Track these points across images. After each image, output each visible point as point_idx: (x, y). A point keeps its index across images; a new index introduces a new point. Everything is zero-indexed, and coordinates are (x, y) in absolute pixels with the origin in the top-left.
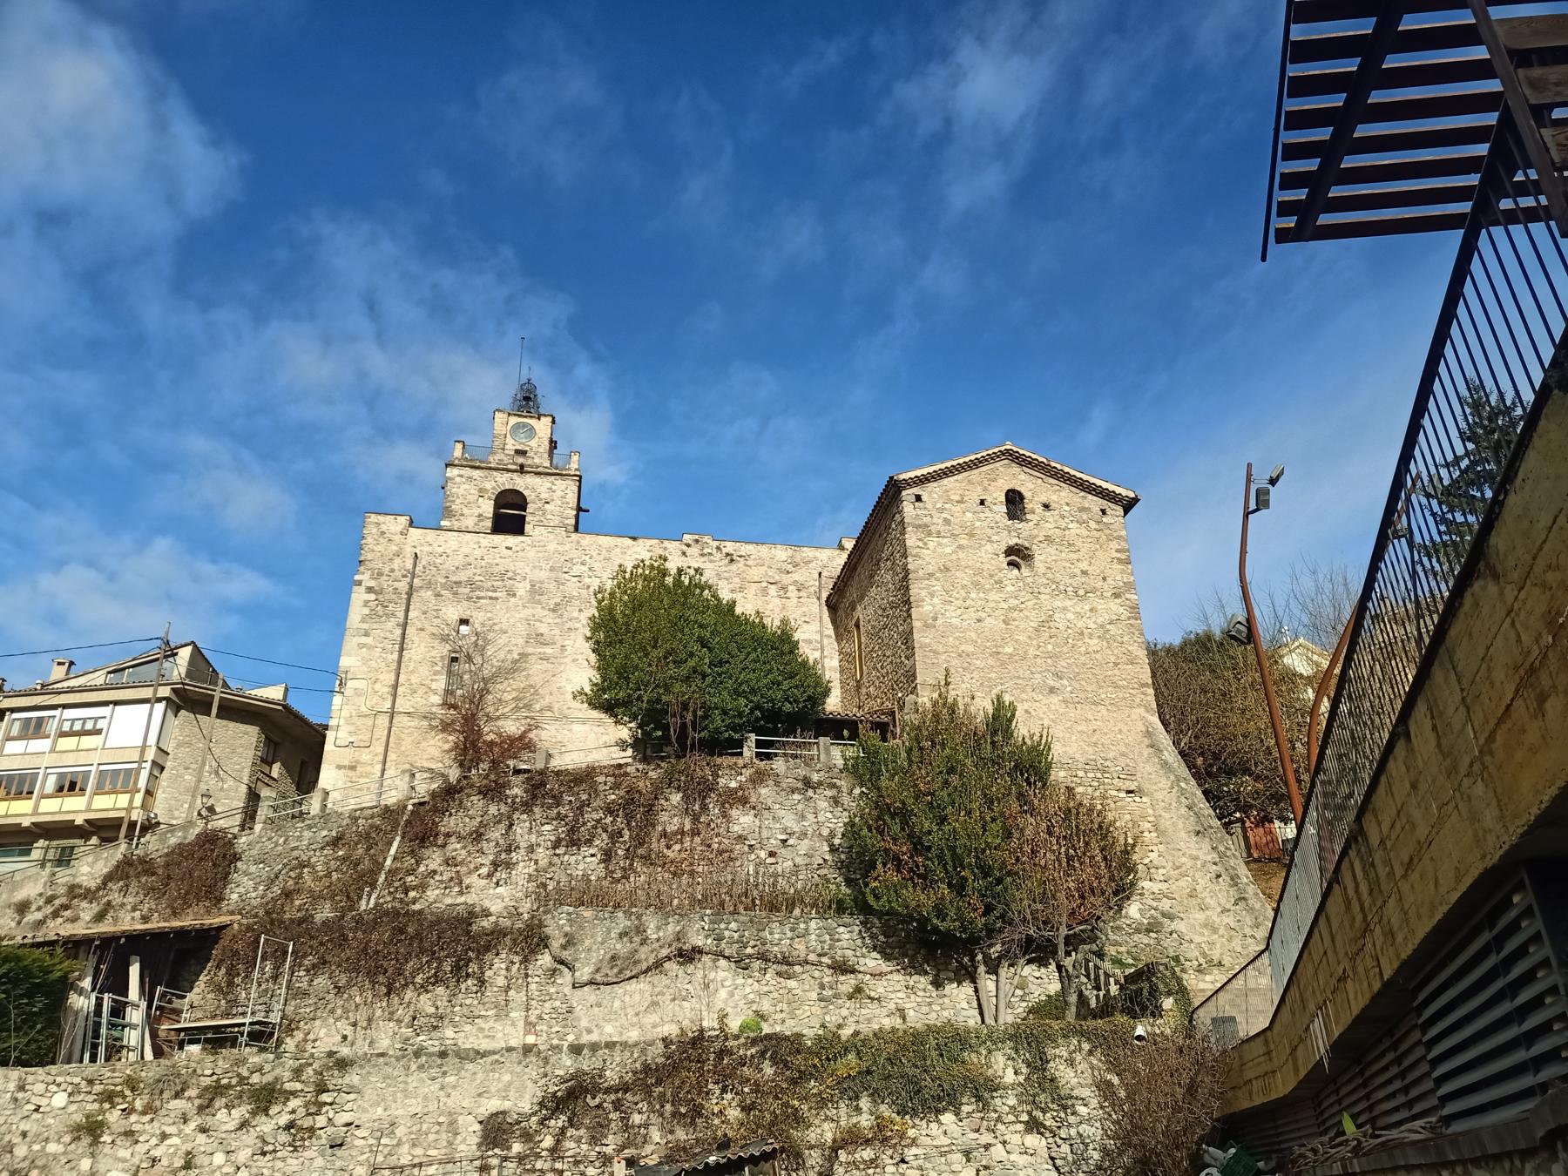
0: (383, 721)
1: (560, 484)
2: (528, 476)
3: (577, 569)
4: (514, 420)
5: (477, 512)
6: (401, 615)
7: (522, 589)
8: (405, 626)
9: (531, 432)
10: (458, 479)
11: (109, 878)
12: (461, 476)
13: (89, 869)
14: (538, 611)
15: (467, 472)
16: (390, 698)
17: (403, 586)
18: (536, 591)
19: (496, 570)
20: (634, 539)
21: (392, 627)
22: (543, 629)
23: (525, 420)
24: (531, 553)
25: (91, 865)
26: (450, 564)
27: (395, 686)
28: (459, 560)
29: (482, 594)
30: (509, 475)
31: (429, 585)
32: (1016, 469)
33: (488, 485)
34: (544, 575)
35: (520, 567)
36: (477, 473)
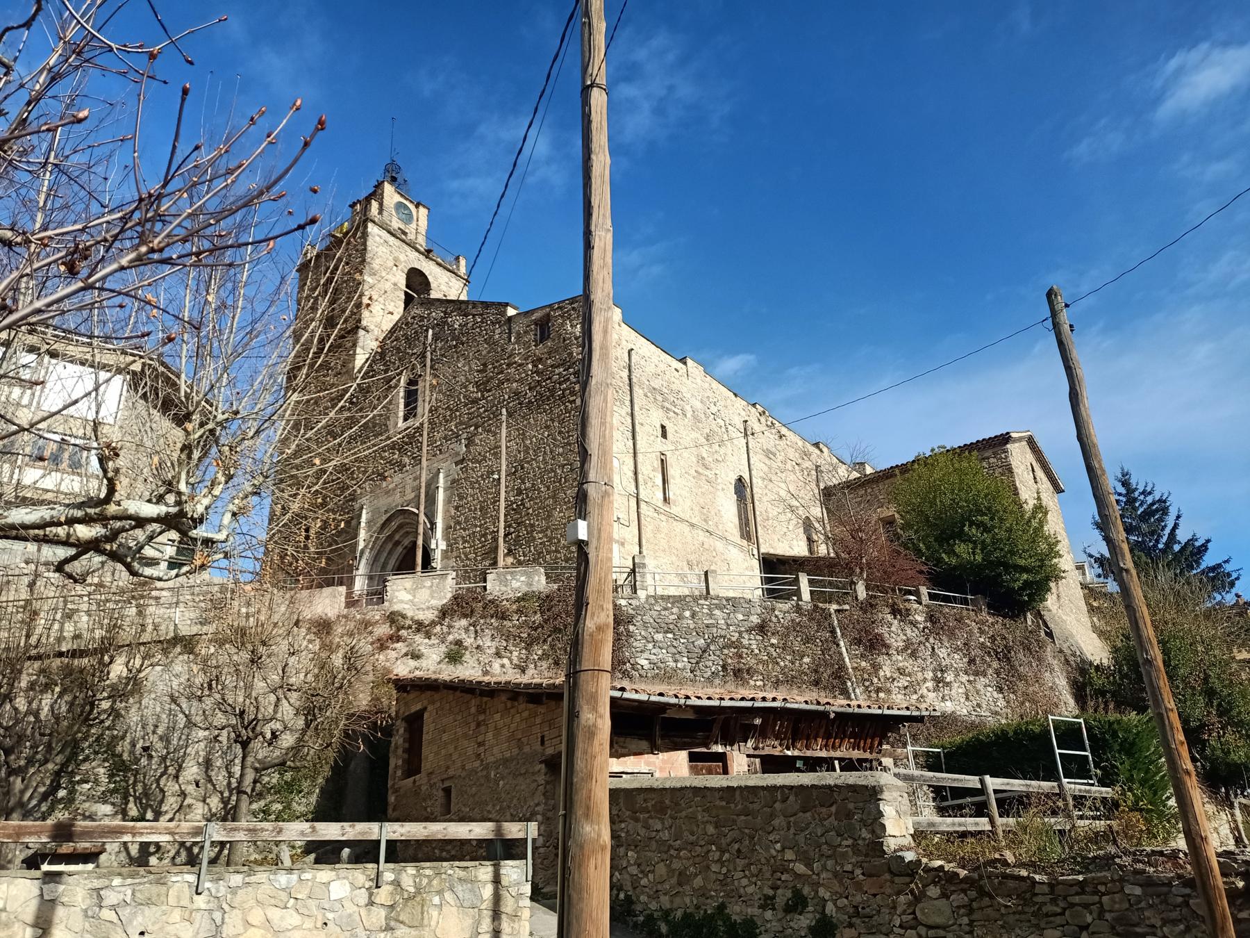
0: (633, 502)
2: (431, 262)
3: (714, 409)
5: (394, 280)
6: (628, 403)
8: (632, 415)
10: (377, 239)
11: (444, 613)
12: (381, 237)
13: (410, 597)
16: (633, 484)
19: (674, 387)
20: (736, 395)
23: (405, 202)
25: (413, 591)
27: (636, 473)
29: (669, 406)
30: (417, 254)
33: (402, 257)
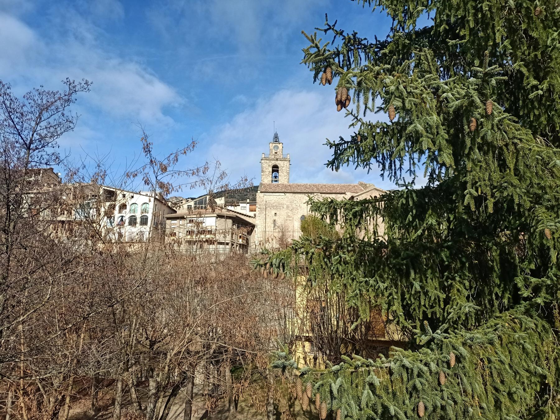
1: (286, 162)
4: (274, 145)
7: (285, 206)
9: (278, 147)
14: (288, 211)
15: (266, 161)
17: (264, 207)
18: (288, 207)
21: (263, 215)
22: (289, 214)
24: (286, 199)
26: (272, 202)
28: (274, 201)
31: (269, 207)
32: (376, 191)
34: (289, 203)
35: (285, 202)
36: (268, 161)
